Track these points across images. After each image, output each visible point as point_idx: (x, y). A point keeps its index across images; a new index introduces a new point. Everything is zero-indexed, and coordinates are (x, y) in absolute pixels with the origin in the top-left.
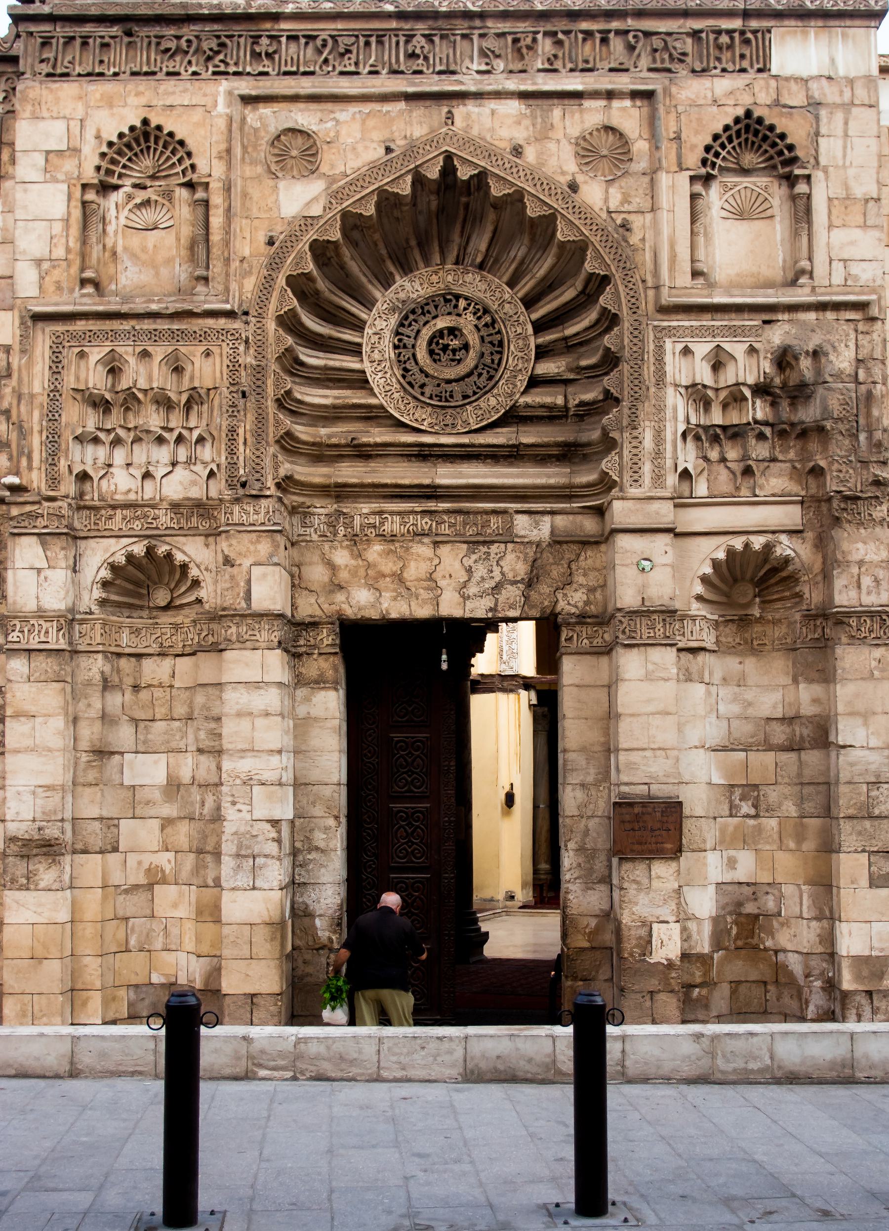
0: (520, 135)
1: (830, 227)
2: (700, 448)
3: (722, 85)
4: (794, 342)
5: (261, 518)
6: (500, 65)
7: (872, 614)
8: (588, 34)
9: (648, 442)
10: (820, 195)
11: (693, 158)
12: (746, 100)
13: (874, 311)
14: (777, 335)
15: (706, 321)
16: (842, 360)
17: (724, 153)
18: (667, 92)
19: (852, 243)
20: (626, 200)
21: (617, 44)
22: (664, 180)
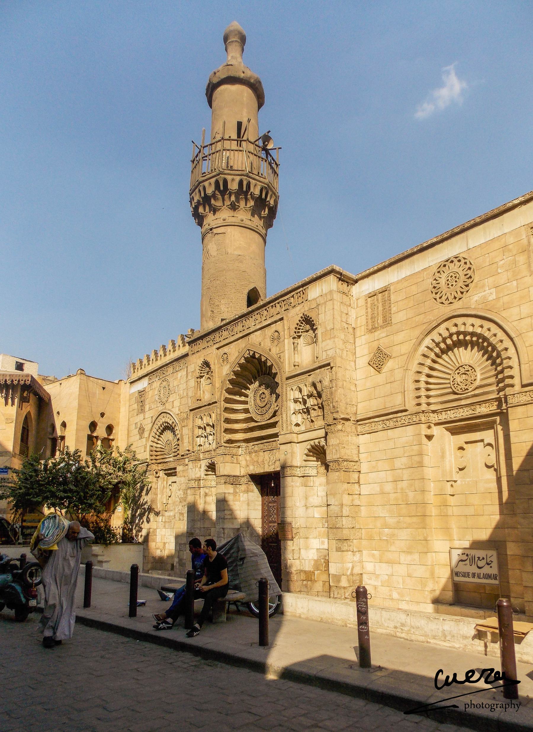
0: (259, 339)
1: (322, 341)
2: (302, 416)
3: (298, 308)
4: (314, 380)
5: (221, 451)
6: (257, 322)
7: (335, 461)
8: (272, 306)
9: (284, 418)
10: (319, 332)
11: (292, 333)
12: (303, 311)
13: (332, 365)
14: (310, 379)
15: (296, 379)
16: (326, 382)
17: (302, 328)
18: (287, 316)
19: (327, 345)
20: (280, 350)
21: (278, 305)
22: (286, 340)
